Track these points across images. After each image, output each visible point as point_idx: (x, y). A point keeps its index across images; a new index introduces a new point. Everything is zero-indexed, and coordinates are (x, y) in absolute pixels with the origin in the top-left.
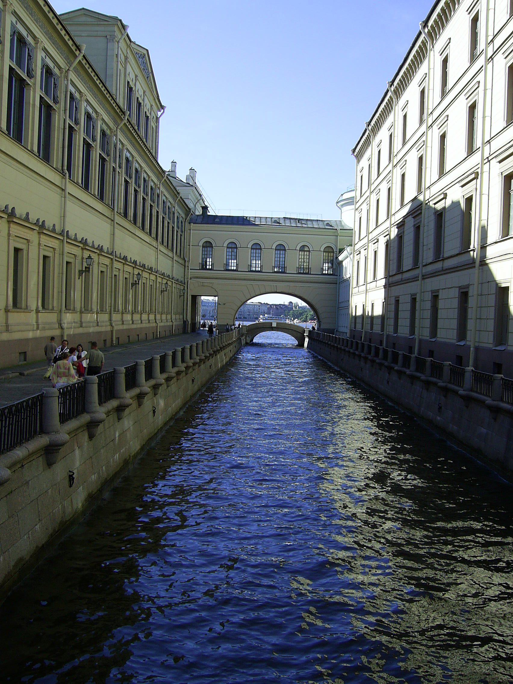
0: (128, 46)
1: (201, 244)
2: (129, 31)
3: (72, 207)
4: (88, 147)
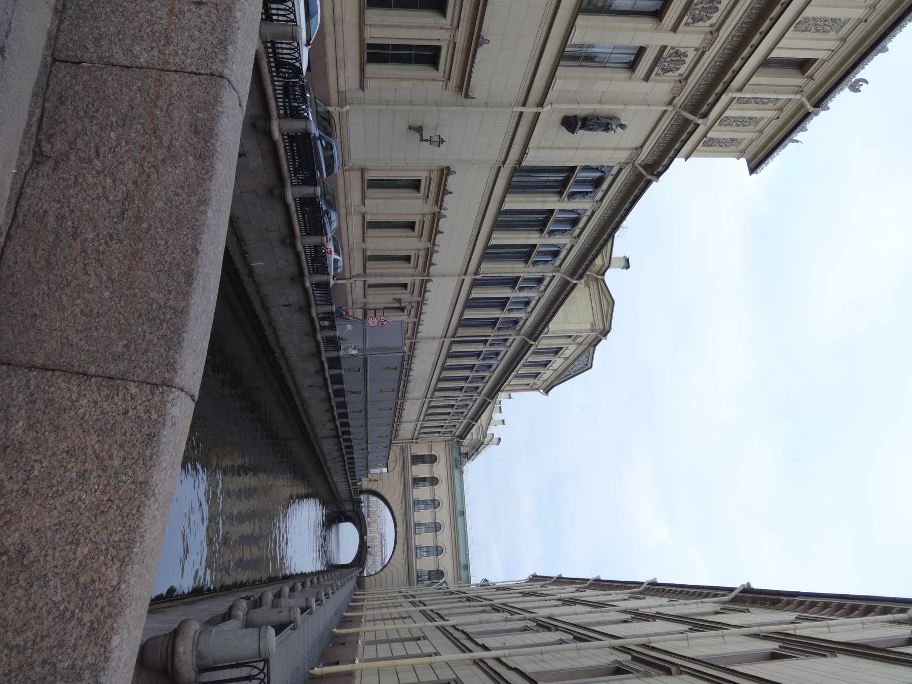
0: (590, 344)
1: (434, 453)
2: (603, 341)
3: (451, 285)
4: (502, 303)
